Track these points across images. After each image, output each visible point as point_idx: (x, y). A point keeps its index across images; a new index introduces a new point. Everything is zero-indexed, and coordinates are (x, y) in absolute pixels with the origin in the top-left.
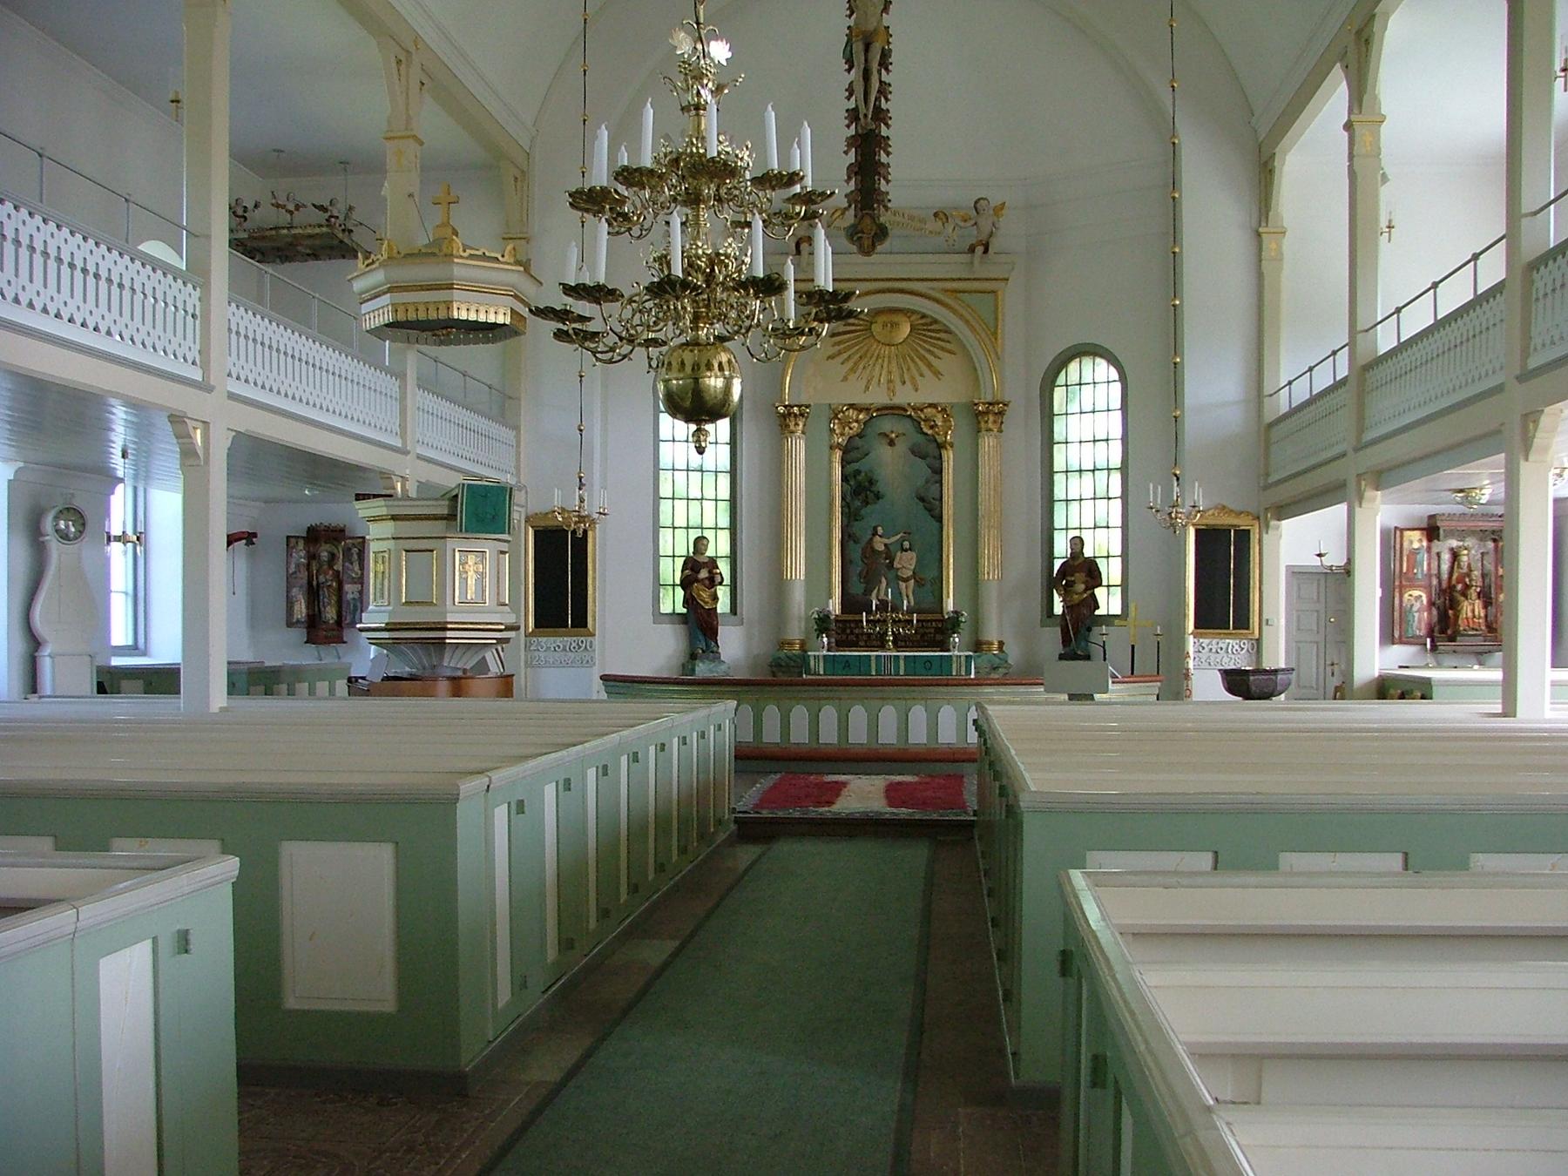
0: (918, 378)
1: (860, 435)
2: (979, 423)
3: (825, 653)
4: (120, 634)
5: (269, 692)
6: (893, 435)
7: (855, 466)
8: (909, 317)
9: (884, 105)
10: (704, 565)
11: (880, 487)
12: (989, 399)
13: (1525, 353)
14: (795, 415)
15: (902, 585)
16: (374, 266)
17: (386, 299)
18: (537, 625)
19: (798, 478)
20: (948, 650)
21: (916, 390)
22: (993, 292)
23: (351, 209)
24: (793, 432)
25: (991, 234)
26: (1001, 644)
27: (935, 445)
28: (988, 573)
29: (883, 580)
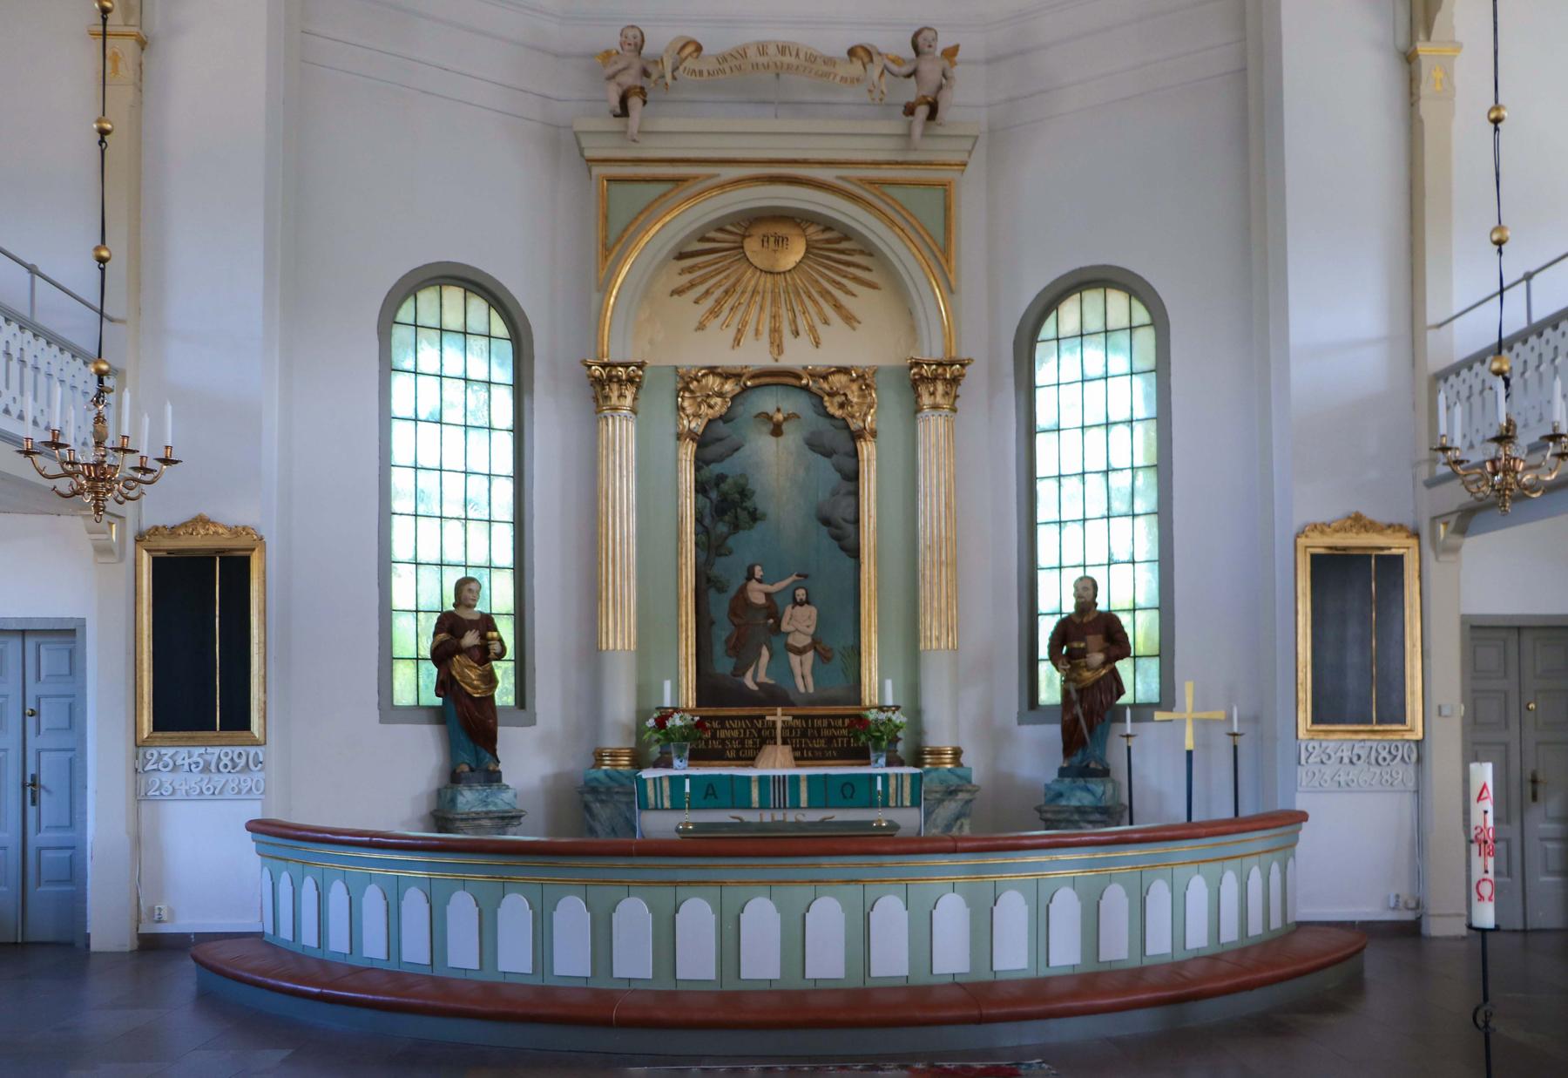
0: (820, 328)
1: (725, 418)
2: (919, 396)
7: (716, 469)
8: (804, 230)
10: (472, 625)
11: (759, 502)
12: (938, 355)
14: (620, 381)
15: (795, 660)
18: (158, 726)
19: (623, 489)
21: (817, 344)
24: (615, 409)
27: (844, 435)
28: (938, 639)
29: (765, 652)
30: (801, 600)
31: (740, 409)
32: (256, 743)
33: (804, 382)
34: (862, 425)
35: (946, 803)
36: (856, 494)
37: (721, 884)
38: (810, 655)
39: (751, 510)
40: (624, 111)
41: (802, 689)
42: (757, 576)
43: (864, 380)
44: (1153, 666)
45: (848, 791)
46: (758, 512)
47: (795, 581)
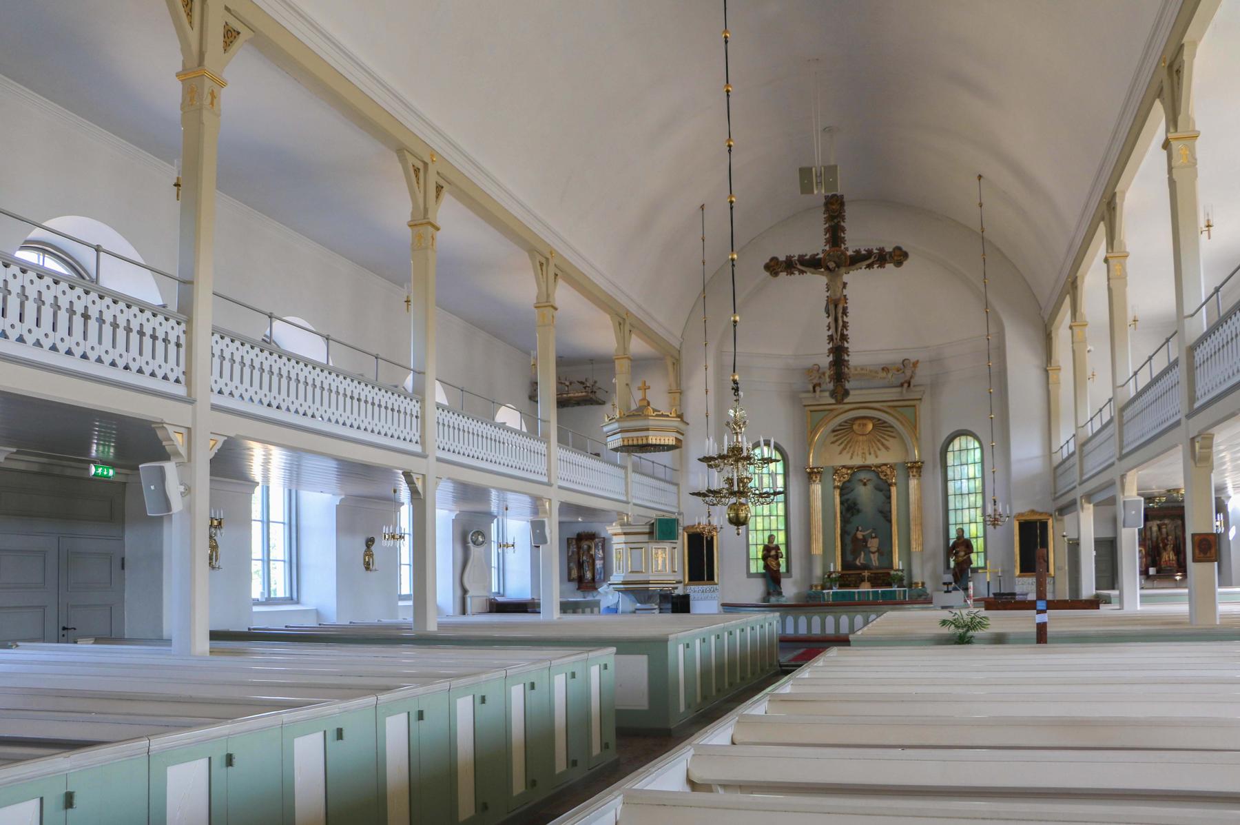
0: (879, 453)
1: (849, 481)
2: (909, 472)
4: (494, 589)
5: (574, 612)
7: (846, 497)
9: (845, 333)
10: (773, 548)
13: (1121, 448)
14: (815, 473)
15: (872, 555)
16: (612, 421)
17: (619, 436)
19: (817, 504)
22: (914, 406)
23: (595, 382)
25: (911, 377)
29: (863, 553)
32: (716, 584)
36: (890, 503)
37: (836, 612)
38: (877, 554)
40: (814, 391)
41: (874, 564)
43: (892, 467)
44: (982, 555)
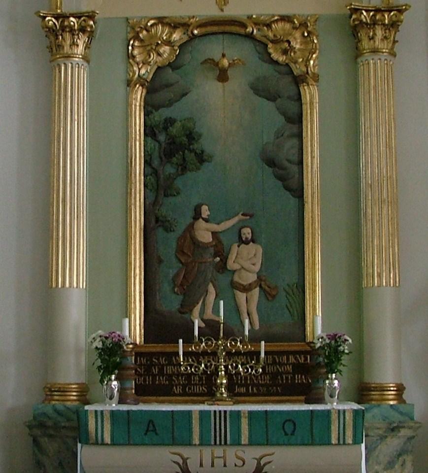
1: (173, 66)
2: (360, 41)
3: (114, 406)
6: (225, 62)
11: (206, 144)
14: (72, 30)
15: (241, 297)
20: (320, 400)
24: (68, 57)
26: (400, 389)
27: (288, 79)
28: (379, 275)
29: (211, 288)
30: (247, 238)
31: (187, 57)
33: (249, 29)
34: (304, 69)
35: (388, 439)
36: (300, 136)
39: (197, 151)
42: (203, 216)
45: (289, 427)
46: (205, 154)
47: (240, 221)
